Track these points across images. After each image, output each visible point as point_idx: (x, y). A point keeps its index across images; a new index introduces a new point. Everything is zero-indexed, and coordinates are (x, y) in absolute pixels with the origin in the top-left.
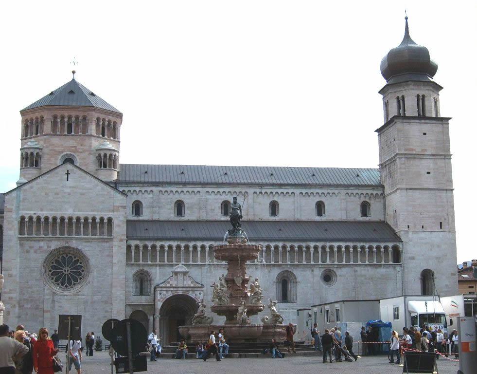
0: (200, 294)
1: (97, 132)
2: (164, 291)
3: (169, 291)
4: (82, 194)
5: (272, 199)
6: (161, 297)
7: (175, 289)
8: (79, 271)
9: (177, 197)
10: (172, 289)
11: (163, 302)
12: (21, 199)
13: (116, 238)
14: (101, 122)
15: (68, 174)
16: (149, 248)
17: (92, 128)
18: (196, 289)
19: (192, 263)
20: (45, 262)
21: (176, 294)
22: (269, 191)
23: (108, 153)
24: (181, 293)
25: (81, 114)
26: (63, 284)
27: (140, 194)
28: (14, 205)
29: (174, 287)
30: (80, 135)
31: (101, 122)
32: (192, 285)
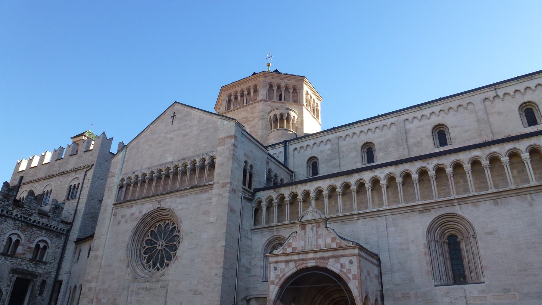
0: (351, 262)
1: (270, 97)
2: (281, 262)
3: (291, 261)
4: (184, 136)
5: (520, 100)
6: (277, 276)
7: (301, 257)
8: (175, 243)
9: (364, 139)
10: (296, 257)
11: (279, 284)
12: (126, 159)
13: (218, 183)
14: (275, 88)
15: (173, 117)
16: (287, 199)
17: (262, 93)
18: (341, 252)
19: (357, 212)
20: (135, 234)
21: (303, 266)
22: (511, 89)
23: (278, 112)
24: (311, 264)
25: (251, 84)
26: (154, 265)
27: (315, 147)
28: (118, 168)
29: (299, 253)
30: (251, 104)
31: (275, 88)
32: (334, 245)
